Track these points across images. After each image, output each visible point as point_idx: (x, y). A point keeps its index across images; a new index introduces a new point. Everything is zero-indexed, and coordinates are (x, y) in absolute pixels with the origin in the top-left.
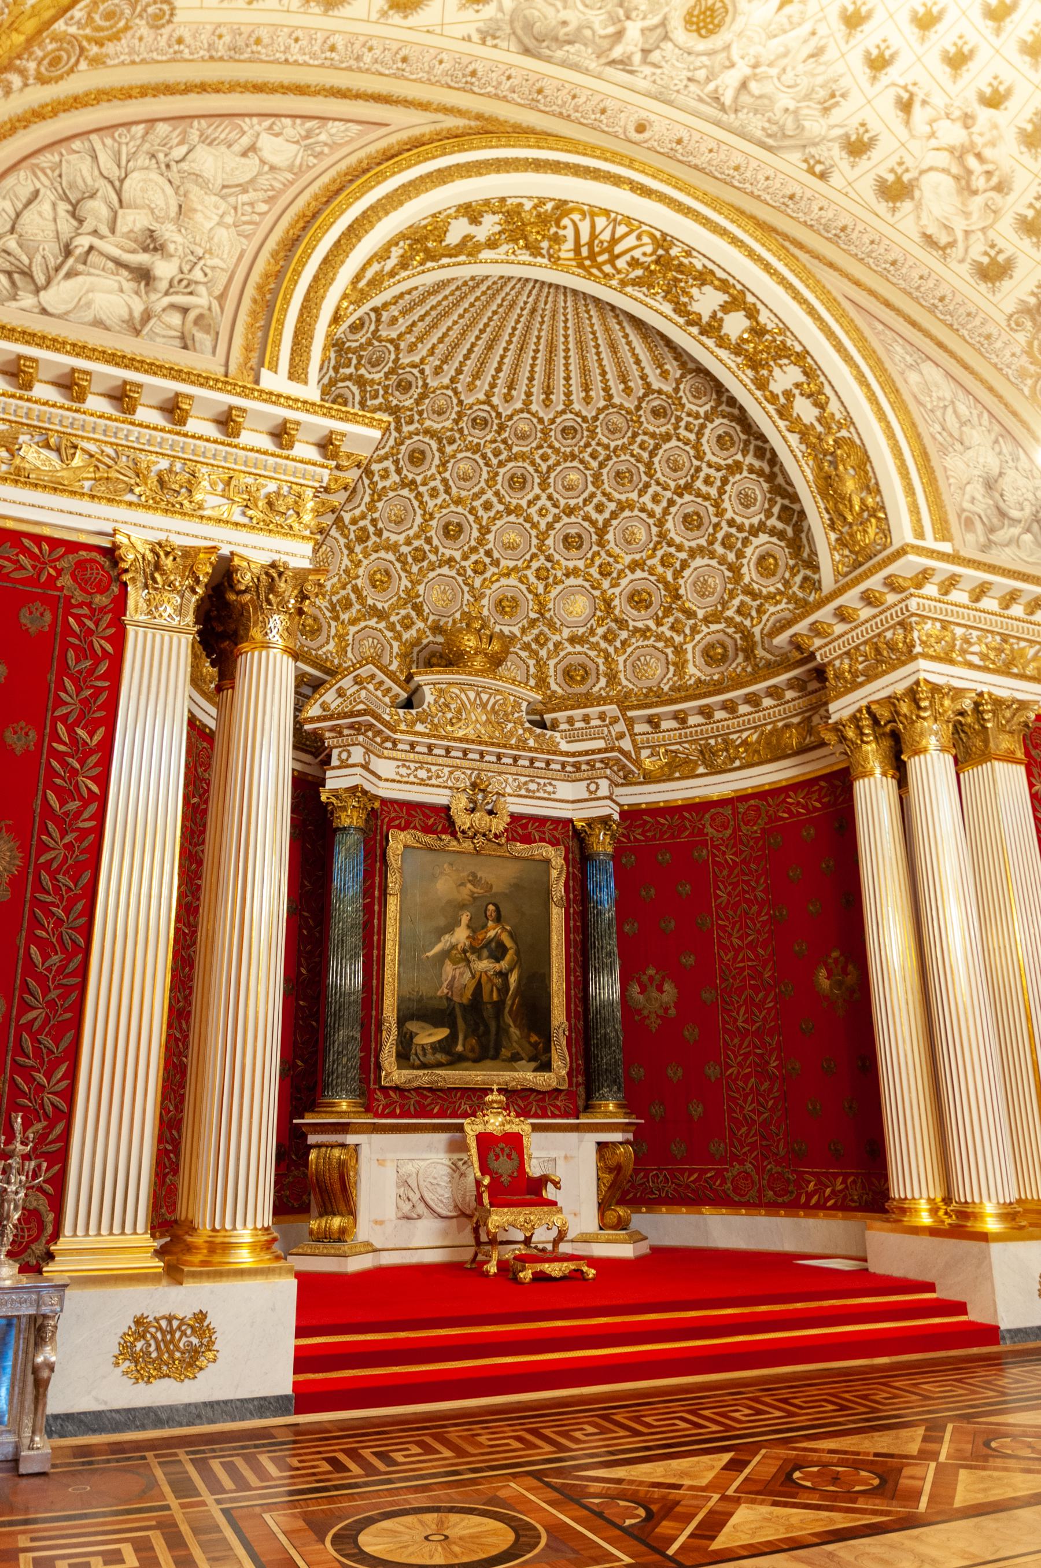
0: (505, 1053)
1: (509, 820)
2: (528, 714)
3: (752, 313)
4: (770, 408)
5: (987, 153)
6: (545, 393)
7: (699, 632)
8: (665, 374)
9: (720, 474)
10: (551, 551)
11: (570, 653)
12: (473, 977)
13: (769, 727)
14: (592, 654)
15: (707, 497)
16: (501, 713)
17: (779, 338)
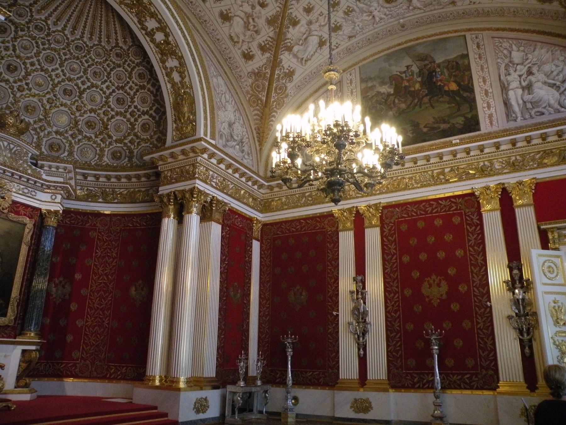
1: (11, 203)
2: (31, 158)
3: (167, 35)
4: (164, 71)
5: (256, 20)
6: (72, 28)
7: (112, 145)
8: (125, 42)
9: (136, 87)
10: (57, 93)
13: (132, 190)
14: (64, 141)
15: (129, 94)
16: (18, 155)
17: (174, 48)
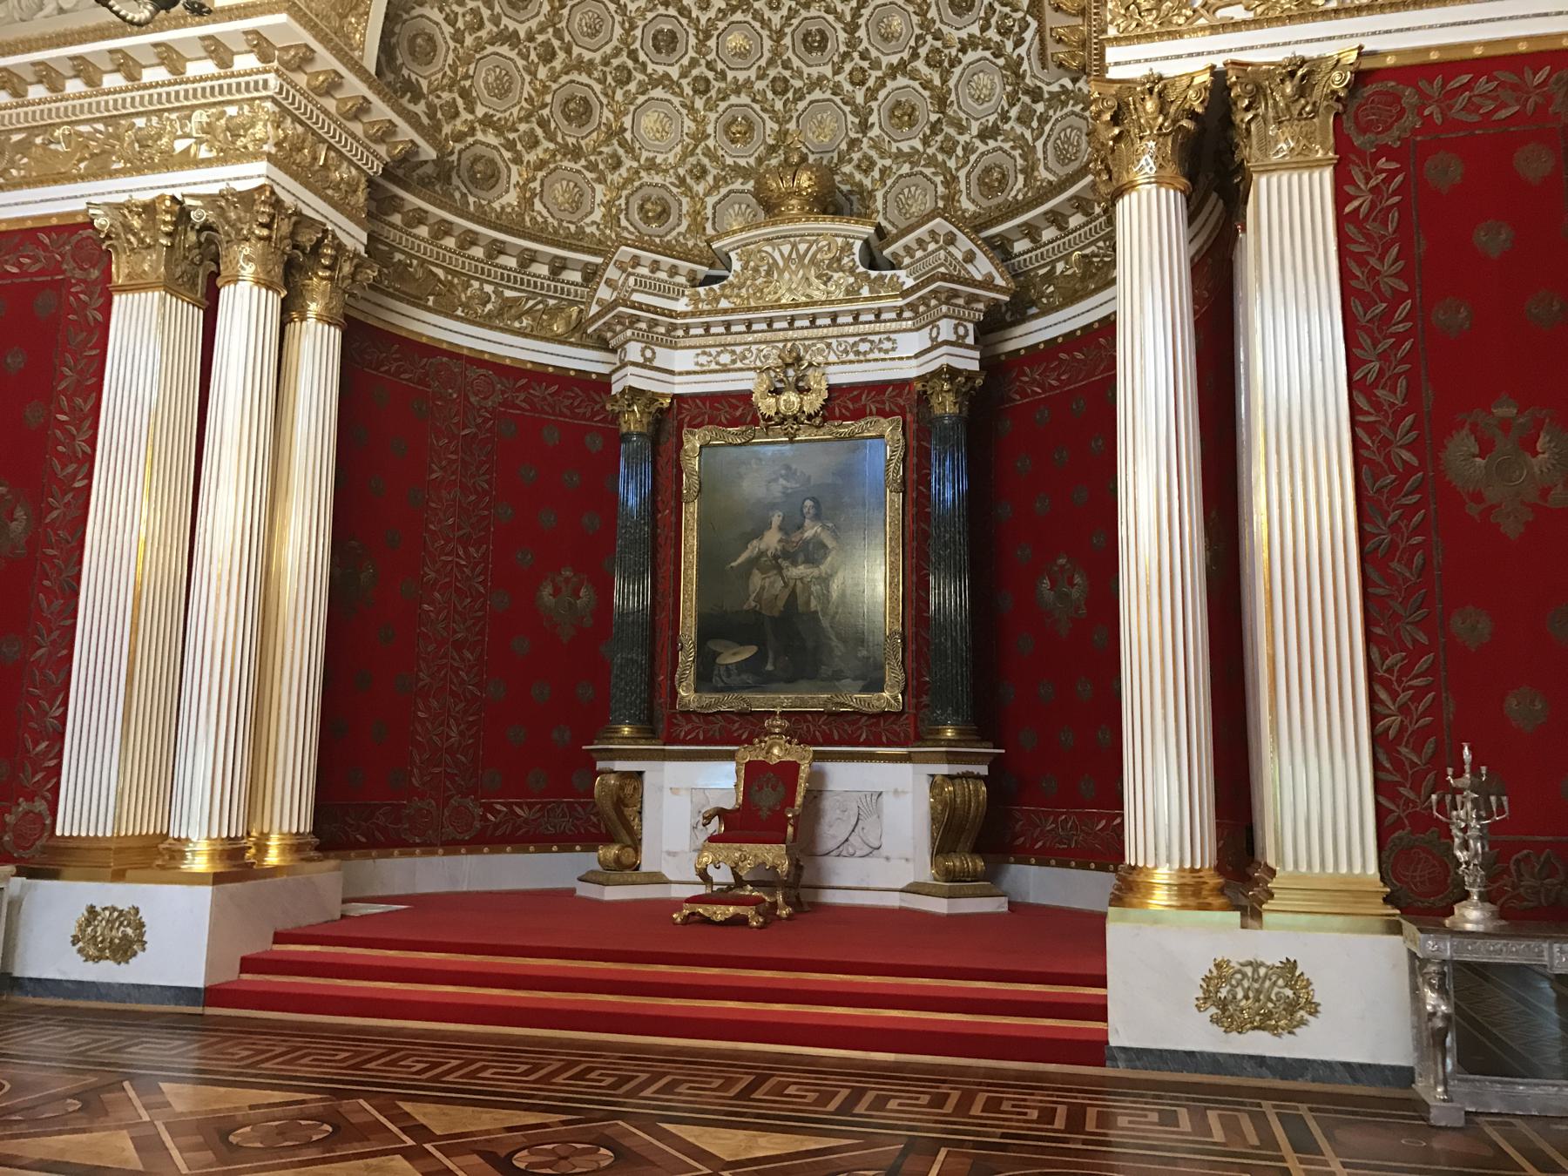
0: (825, 670)
11: (983, 154)
12: (786, 585)
14: (1007, 146)
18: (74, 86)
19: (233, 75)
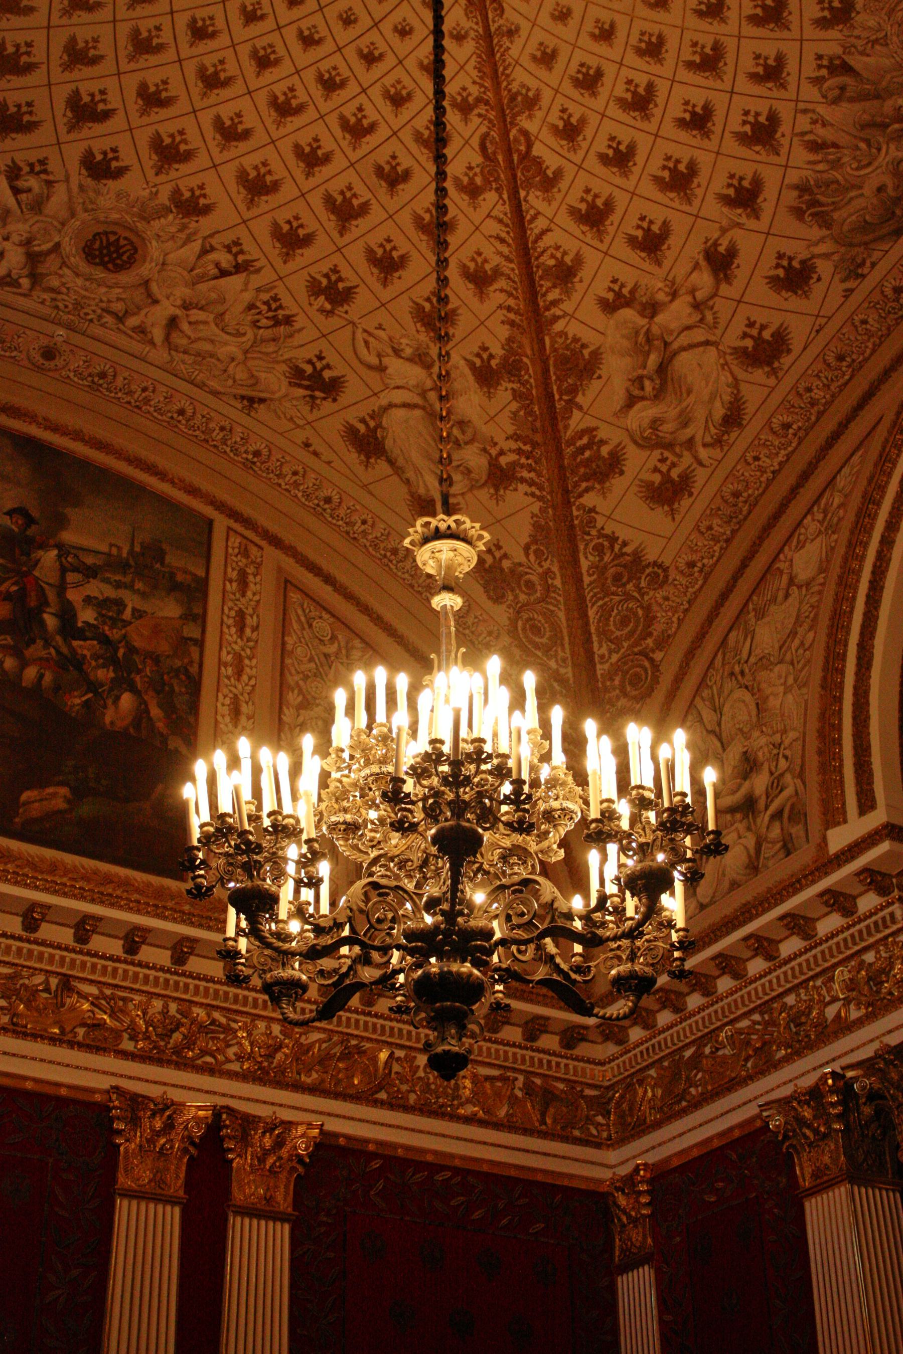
18: (724, 984)
19: (860, 920)
